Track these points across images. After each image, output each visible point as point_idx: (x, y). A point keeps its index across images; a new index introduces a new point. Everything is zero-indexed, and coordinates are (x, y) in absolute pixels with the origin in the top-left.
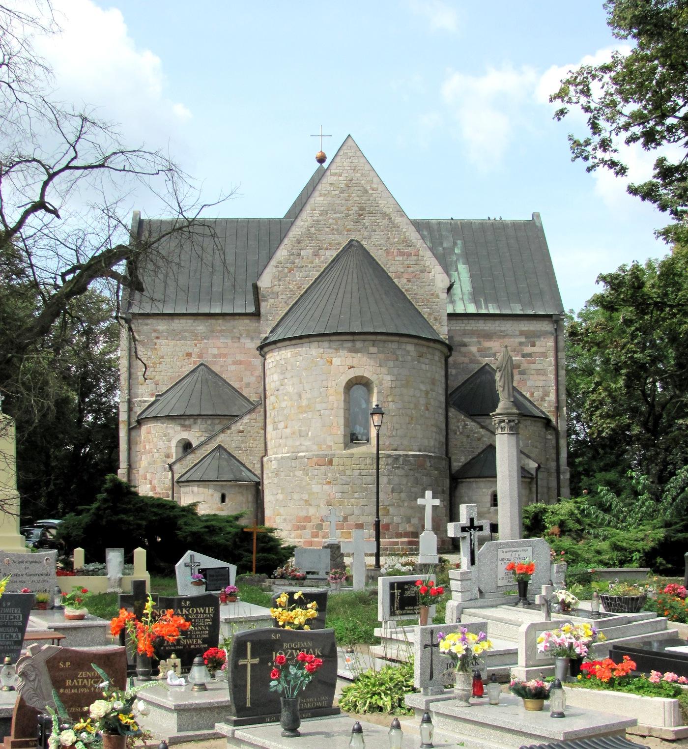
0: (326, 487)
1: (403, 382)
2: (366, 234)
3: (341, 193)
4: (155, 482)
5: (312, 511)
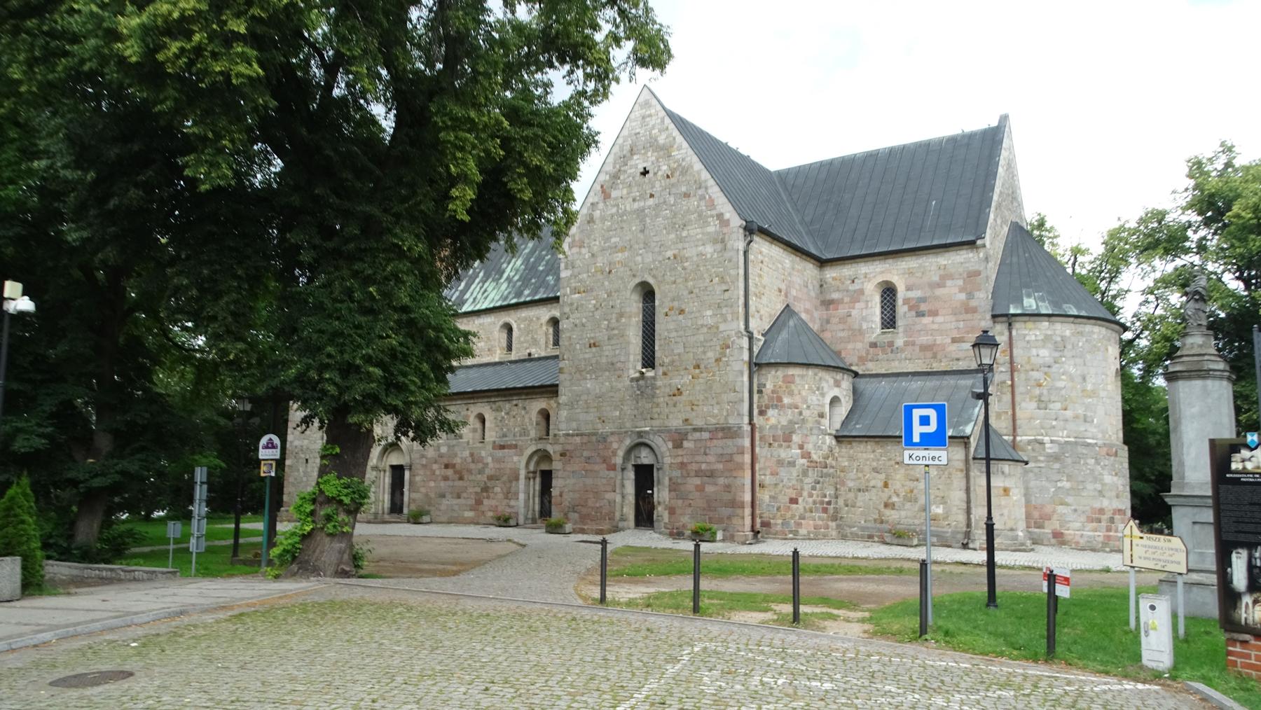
0: (1115, 479)
4: (809, 447)
5: (1105, 503)
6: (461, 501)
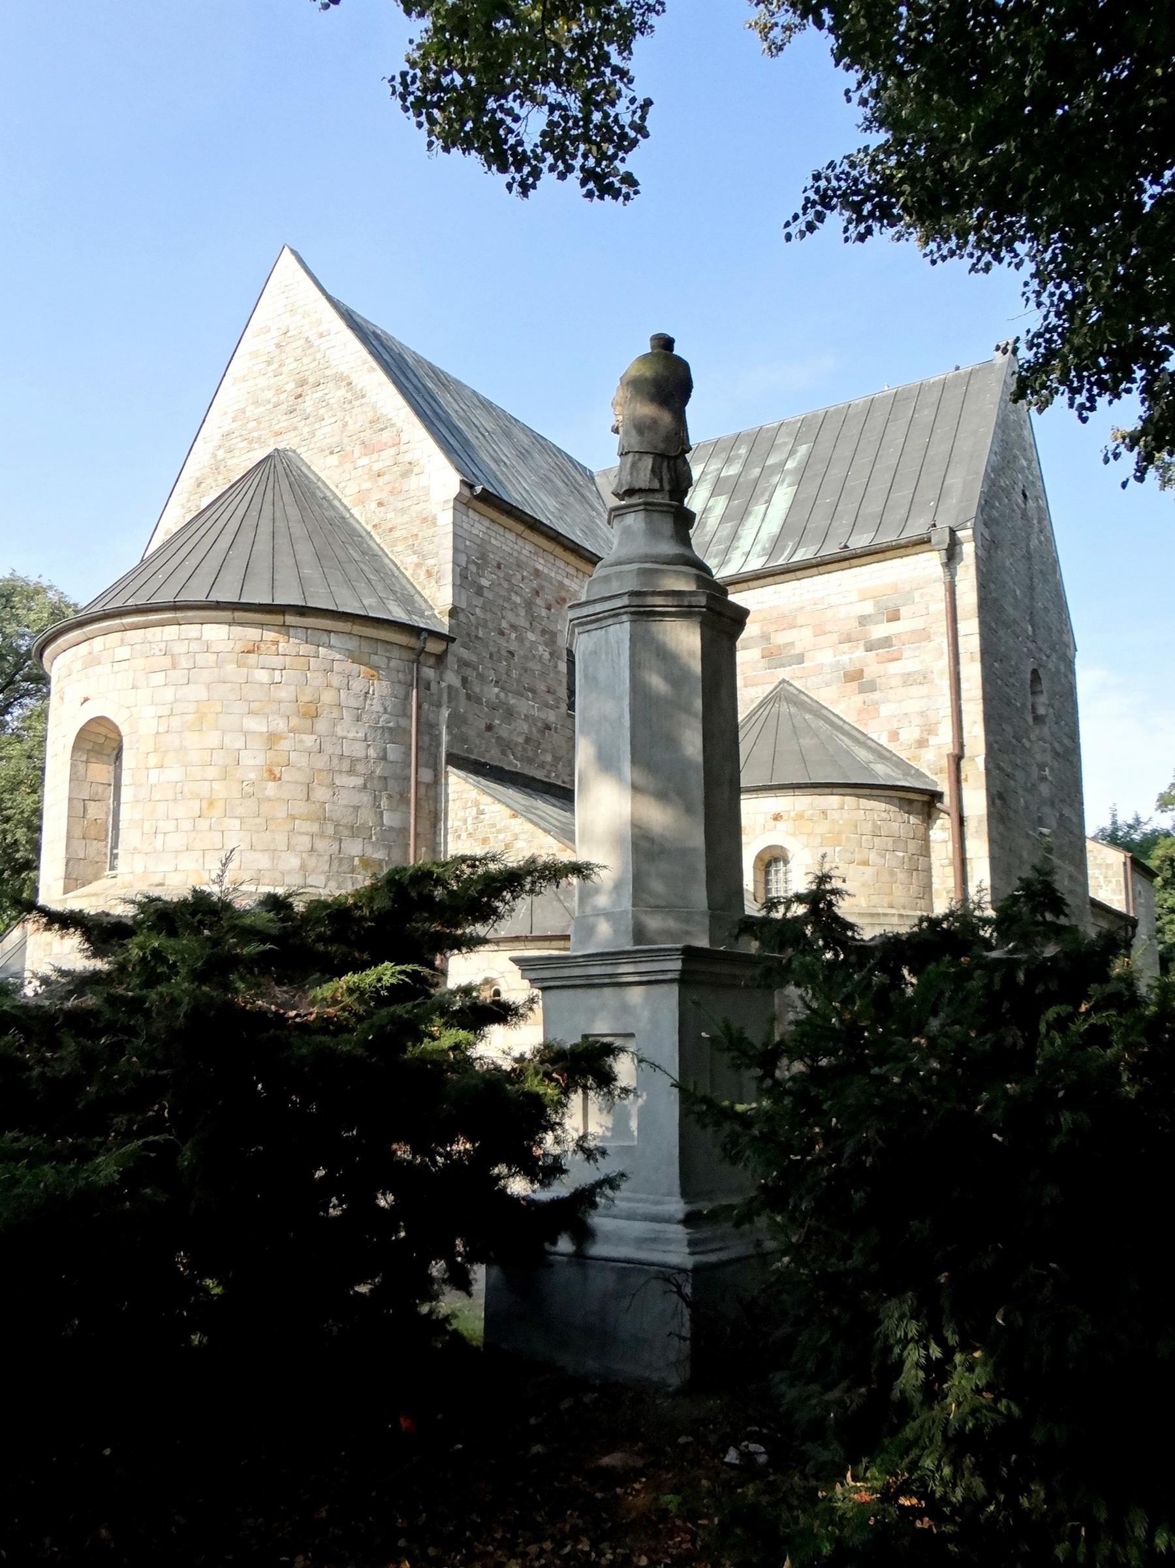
1: (190, 718)
2: (306, 430)
3: (269, 363)
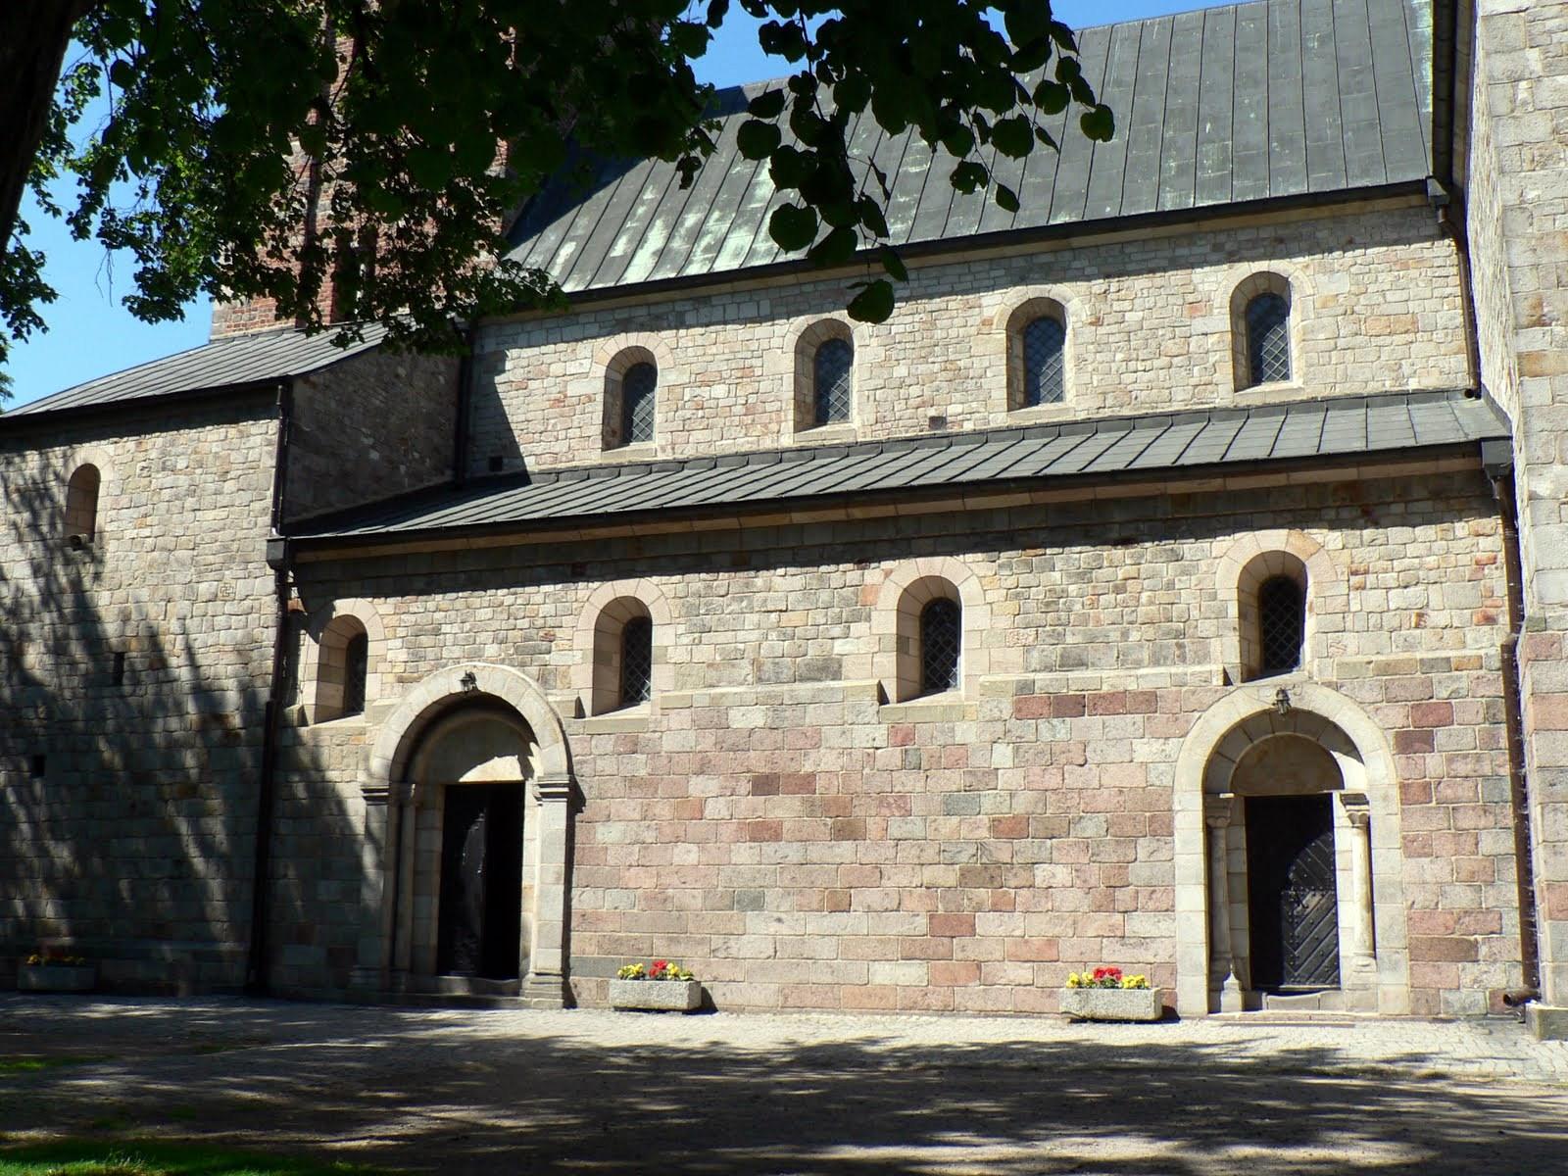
6: (854, 922)
